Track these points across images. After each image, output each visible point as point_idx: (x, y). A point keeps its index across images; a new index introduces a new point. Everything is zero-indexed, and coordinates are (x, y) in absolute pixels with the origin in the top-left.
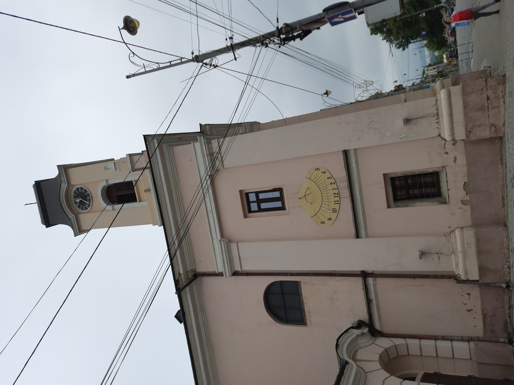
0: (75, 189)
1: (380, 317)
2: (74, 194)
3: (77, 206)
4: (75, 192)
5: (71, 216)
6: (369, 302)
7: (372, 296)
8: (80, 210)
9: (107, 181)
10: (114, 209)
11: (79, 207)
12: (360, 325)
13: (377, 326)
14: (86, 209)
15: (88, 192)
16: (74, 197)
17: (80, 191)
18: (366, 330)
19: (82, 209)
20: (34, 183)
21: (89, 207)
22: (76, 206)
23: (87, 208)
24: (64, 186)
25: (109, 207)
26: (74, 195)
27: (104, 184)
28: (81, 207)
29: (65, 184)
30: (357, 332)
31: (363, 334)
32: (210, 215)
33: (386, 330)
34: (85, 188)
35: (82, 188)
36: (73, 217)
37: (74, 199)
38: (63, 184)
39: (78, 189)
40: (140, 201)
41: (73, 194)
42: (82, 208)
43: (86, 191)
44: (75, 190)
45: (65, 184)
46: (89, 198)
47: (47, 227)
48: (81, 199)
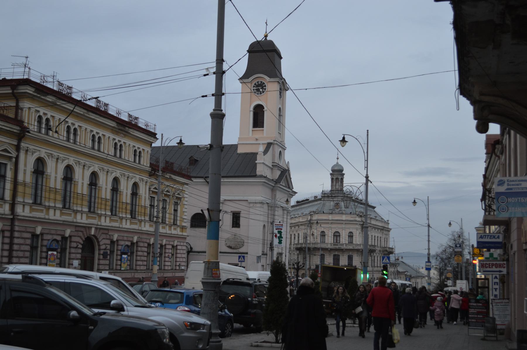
0: (266, 84)
1: (194, 255)
4: (264, 83)
5: (251, 79)
6: (199, 252)
7: (200, 254)
8: (253, 85)
9: (266, 110)
10: (250, 111)
11: (255, 84)
12: (191, 248)
13: (191, 254)
16: (261, 82)
18: (189, 250)
22: (255, 82)
24: (268, 79)
25: (252, 109)
27: (265, 108)
30: (189, 247)
31: (189, 249)
32: (233, 197)
33: (189, 256)
35: (265, 89)
39: (265, 86)
40: (252, 130)
41: (263, 81)
44: (264, 84)
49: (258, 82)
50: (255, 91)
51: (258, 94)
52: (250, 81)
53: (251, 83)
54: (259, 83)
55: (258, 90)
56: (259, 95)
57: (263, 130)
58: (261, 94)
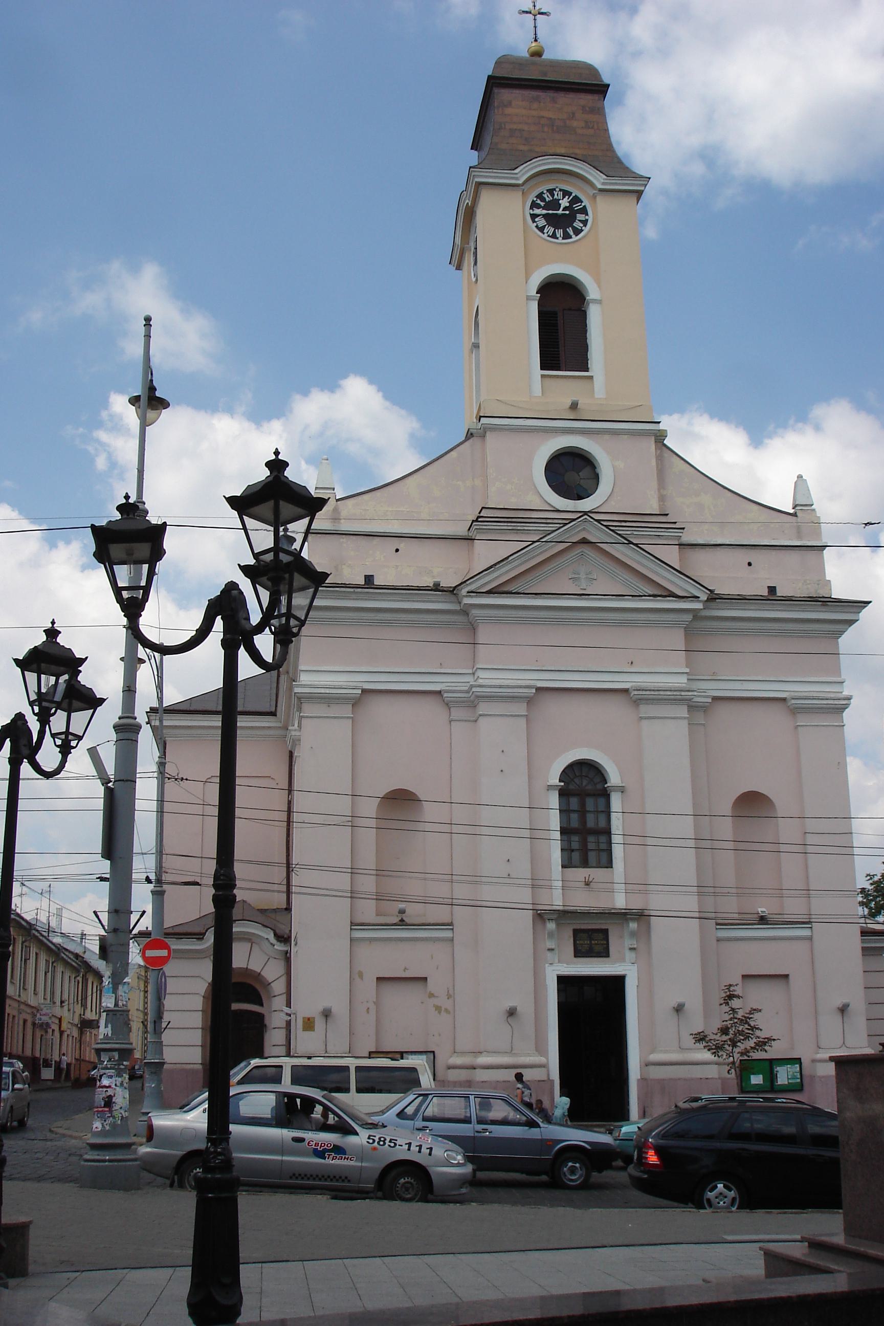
0: (586, 203)
2: (573, 195)
3: (542, 193)
8: (532, 197)
9: (598, 302)
10: (529, 298)
11: (540, 196)
14: (534, 217)
15: (574, 238)
16: (566, 193)
17: (581, 217)
19: (534, 205)
20: (606, 80)
21: (537, 227)
23: (536, 220)
24: (598, 179)
27: (593, 292)
28: (539, 202)
29: (603, 184)
34: (586, 230)
35: (585, 223)
36: (517, 179)
37: (560, 190)
38: (604, 179)
39: (584, 211)
40: (543, 376)
42: (538, 207)
43: (577, 232)
44: (582, 202)
45: (603, 184)
46: (558, 236)
47: (489, 76)
48: (560, 212)
49: (551, 191)
50: (542, 222)
51: (554, 236)
52: (520, 182)
54: (556, 196)
55: (554, 221)
56: (560, 240)
57: (591, 378)
58: (566, 236)
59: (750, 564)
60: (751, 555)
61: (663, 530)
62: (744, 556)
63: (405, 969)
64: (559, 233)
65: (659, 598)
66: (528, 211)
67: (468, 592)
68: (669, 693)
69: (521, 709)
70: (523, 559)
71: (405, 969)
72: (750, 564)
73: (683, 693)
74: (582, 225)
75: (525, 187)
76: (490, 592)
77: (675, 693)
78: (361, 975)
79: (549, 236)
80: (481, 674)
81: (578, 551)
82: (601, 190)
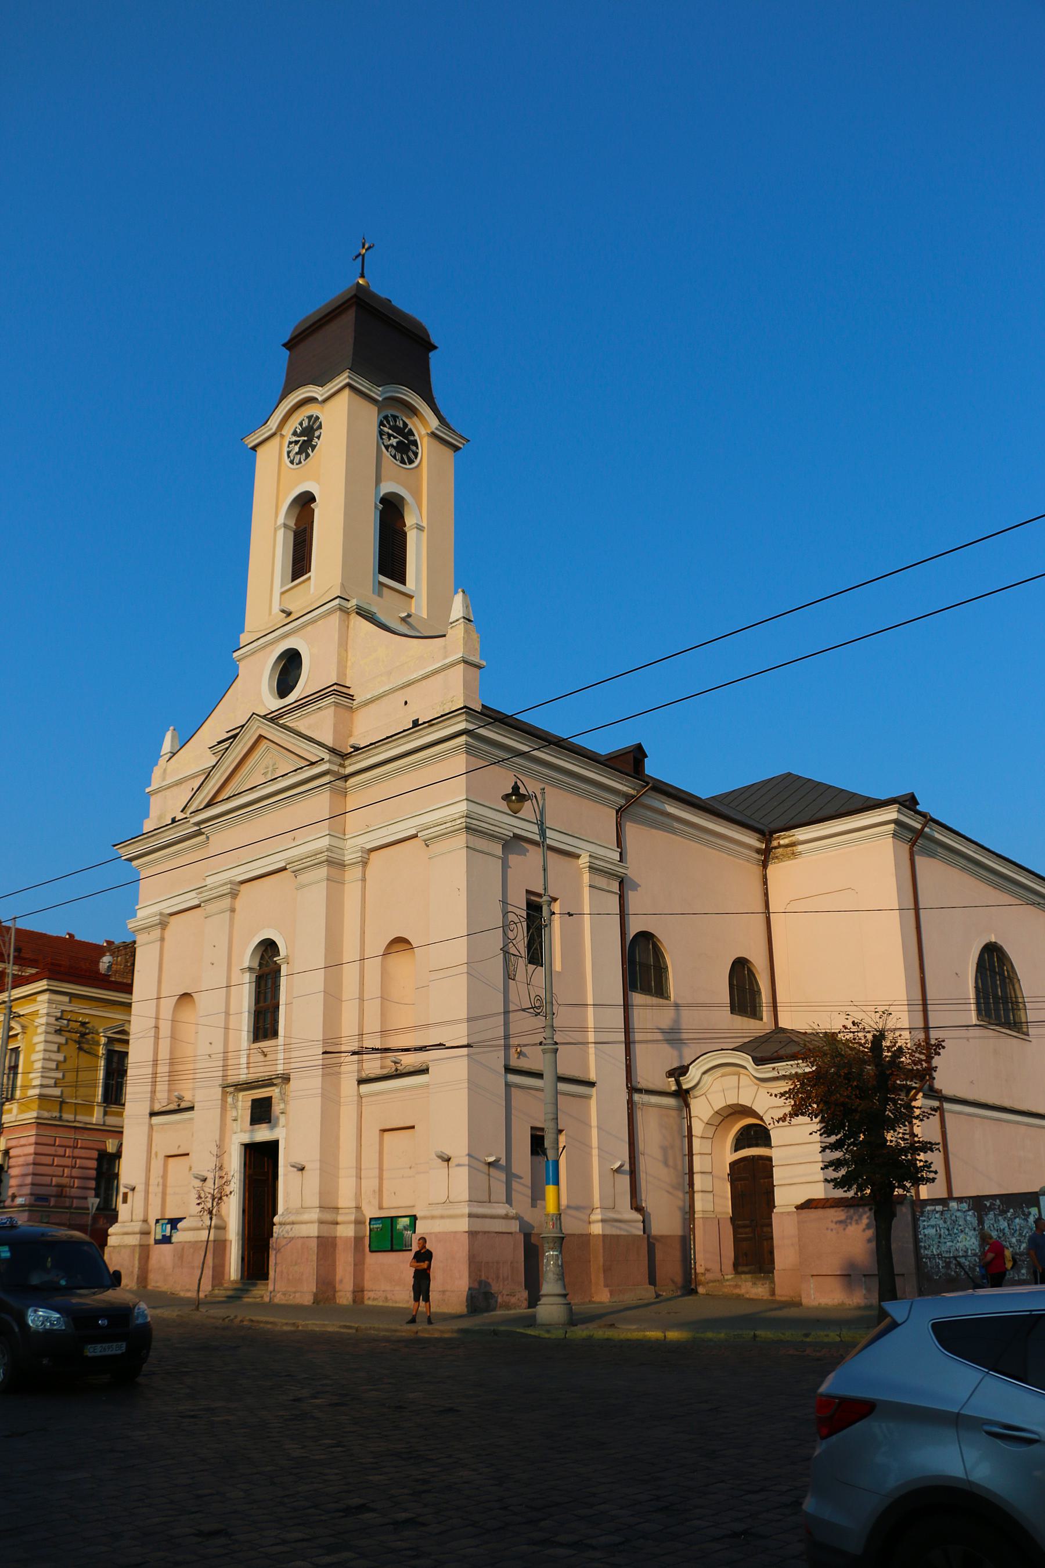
16: (310, 418)
24: (318, 392)
26: (312, 416)
29: (322, 395)
35: (318, 437)
36: (271, 429)
43: (314, 448)
53: (282, 436)
59: (406, 703)
60: (407, 694)
61: (320, 702)
62: (400, 697)
63: (179, 1147)
64: (303, 456)
65: (298, 771)
66: (286, 450)
67: (191, 813)
68: (309, 859)
69: (226, 902)
70: (221, 771)
71: (179, 1147)
72: (406, 703)
73: (318, 856)
74: (316, 440)
75: (284, 432)
76: (209, 805)
77: (313, 858)
78: (156, 1153)
79: (297, 464)
80: (209, 881)
81: (265, 747)
82: (325, 401)
